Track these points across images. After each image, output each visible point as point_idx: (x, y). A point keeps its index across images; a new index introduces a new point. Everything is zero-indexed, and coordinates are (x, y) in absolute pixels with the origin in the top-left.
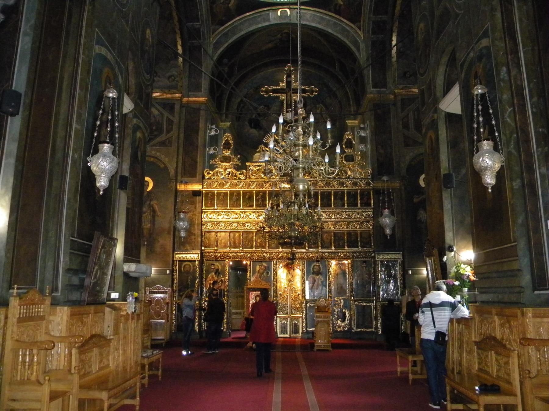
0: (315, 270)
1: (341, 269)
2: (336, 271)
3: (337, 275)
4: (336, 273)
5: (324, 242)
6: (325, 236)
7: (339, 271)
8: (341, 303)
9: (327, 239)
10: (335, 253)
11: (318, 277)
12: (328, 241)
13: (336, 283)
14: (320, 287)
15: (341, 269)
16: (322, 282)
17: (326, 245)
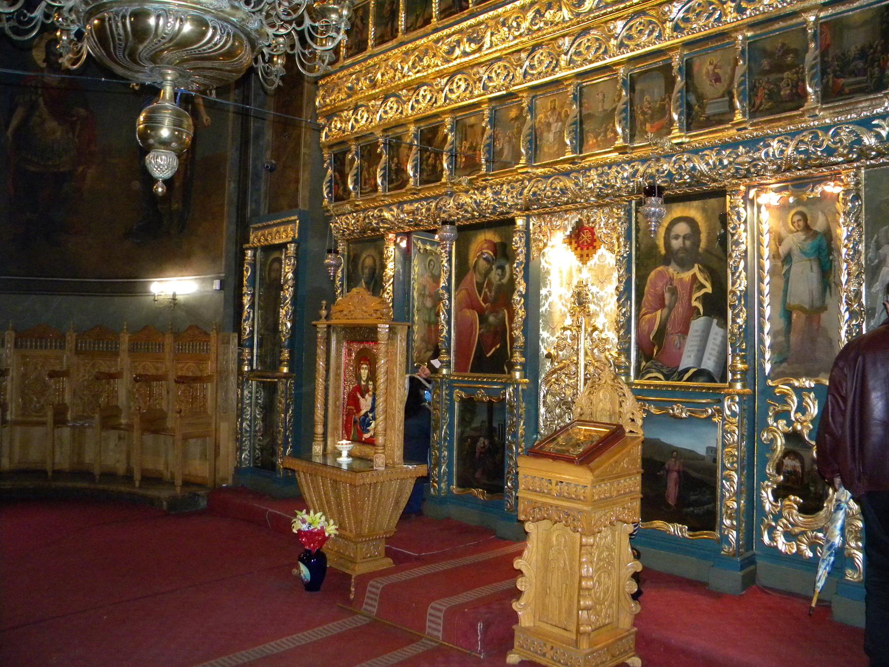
0: (676, 244)
1: (807, 228)
2: (780, 240)
3: (788, 259)
4: (783, 250)
5: (700, 98)
6: (704, 68)
7: (794, 240)
8: (802, 409)
9: (718, 79)
10: (752, 144)
11: (687, 276)
12: (721, 87)
13: (779, 308)
14: (697, 324)
15: (807, 228)
16: (705, 298)
17: (709, 111)
